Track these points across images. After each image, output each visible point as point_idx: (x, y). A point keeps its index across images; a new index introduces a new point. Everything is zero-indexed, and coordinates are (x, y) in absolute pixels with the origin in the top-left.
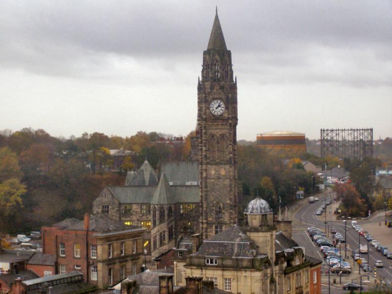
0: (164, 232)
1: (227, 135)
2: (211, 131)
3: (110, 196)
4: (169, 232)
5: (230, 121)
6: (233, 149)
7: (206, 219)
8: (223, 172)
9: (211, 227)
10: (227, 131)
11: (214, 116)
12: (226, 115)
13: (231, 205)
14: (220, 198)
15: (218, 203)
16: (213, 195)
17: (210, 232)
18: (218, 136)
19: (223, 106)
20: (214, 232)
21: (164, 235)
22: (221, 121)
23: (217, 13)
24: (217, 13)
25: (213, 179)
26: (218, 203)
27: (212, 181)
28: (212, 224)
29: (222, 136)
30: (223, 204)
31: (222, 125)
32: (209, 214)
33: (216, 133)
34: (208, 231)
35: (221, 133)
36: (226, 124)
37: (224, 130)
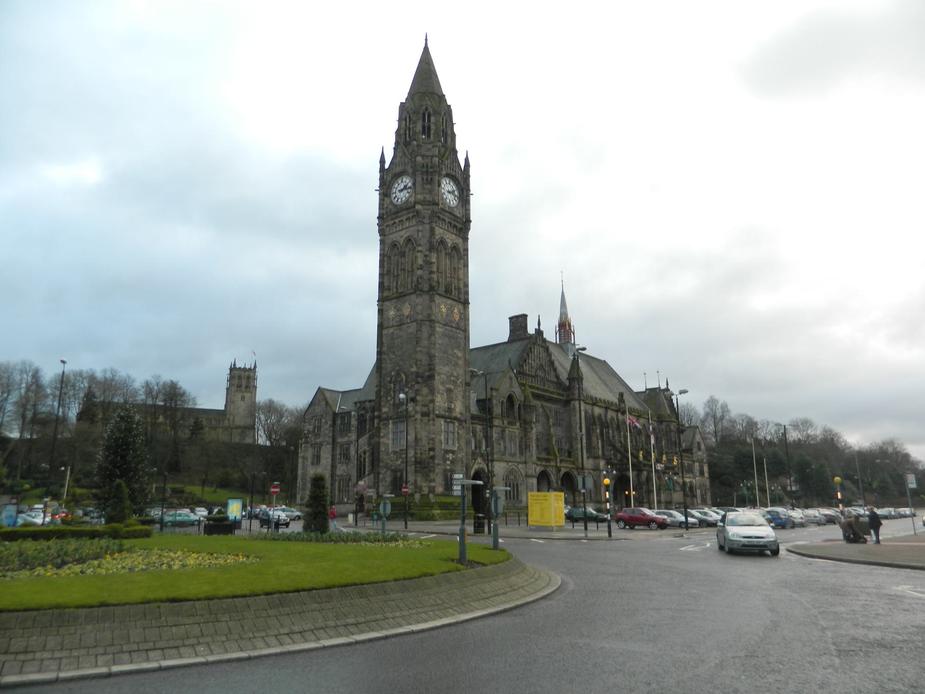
0: (365, 453)
1: (415, 236)
2: (391, 236)
3: (323, 403)
4: (372, 454)
5: (418, 207)
6: (424, 261)
7: (380, 410)
8: (406, 311)
9: (386, 425)
10: (415, 228)
11: (396, 206)
12: (412, 199)
13: (417, 375)
14: (401, 363)
15: (398, 374)
16: (391, 359)
17: (383, 437)
18: (402, 240)
19: (410, 185)
20: (391, 436)
21: (365, 459)
22: (405, 212)
23: (426, 40)
24: (426, 40)
25: (393, 326)
26: (398, 374)
27: (391, 330)
28: (388, 419)
29: (408, 240)
30: (405, 374)
31: (408, 219)
32: (384, 399)
33: (399, 239)
34: (382, 434)
35: (406, 236)
36: (413, 217)
37: (411, 229)
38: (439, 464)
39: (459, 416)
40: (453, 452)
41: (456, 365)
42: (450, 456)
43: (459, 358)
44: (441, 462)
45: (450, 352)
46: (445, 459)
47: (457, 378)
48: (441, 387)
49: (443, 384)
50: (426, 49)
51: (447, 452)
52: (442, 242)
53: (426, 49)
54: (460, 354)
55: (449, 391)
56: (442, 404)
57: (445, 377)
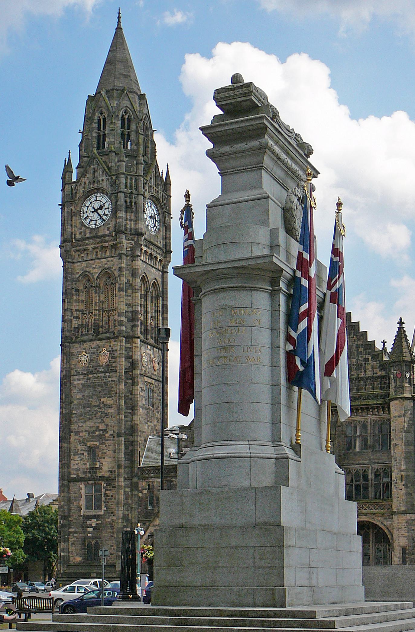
23: (119, 17)
24: (119, 17)
38: (76, 532)
39: (107, 474)
40: (97, 517)
41: (106, 415)
42: (94, 522)
43: (110, 406)
44: (80, 530)
45: (95, 402)
46: (84, 527)
47: (105, 431)
48: (79, 447)
49: (82, 443)
50: (119, 29)
51: (89, 518)
52: (85, 275)
53: (119, 29)
54: (110, 401)
55: (92, 451)
56: (81, 466)
57: (86, 435)
